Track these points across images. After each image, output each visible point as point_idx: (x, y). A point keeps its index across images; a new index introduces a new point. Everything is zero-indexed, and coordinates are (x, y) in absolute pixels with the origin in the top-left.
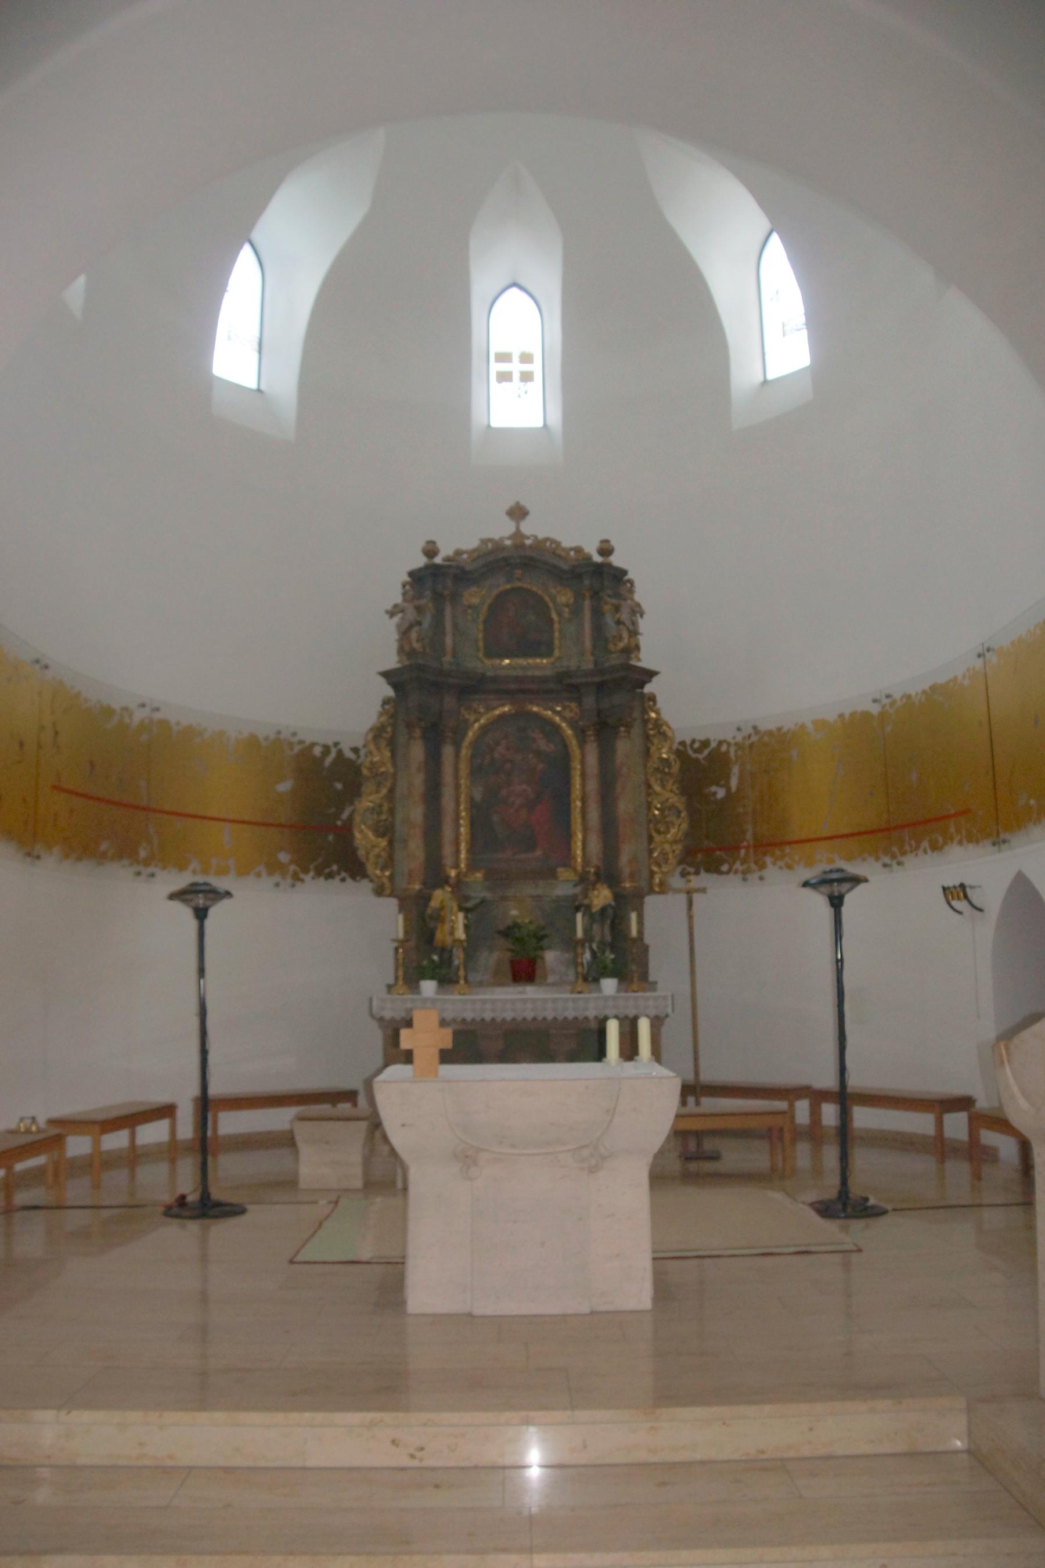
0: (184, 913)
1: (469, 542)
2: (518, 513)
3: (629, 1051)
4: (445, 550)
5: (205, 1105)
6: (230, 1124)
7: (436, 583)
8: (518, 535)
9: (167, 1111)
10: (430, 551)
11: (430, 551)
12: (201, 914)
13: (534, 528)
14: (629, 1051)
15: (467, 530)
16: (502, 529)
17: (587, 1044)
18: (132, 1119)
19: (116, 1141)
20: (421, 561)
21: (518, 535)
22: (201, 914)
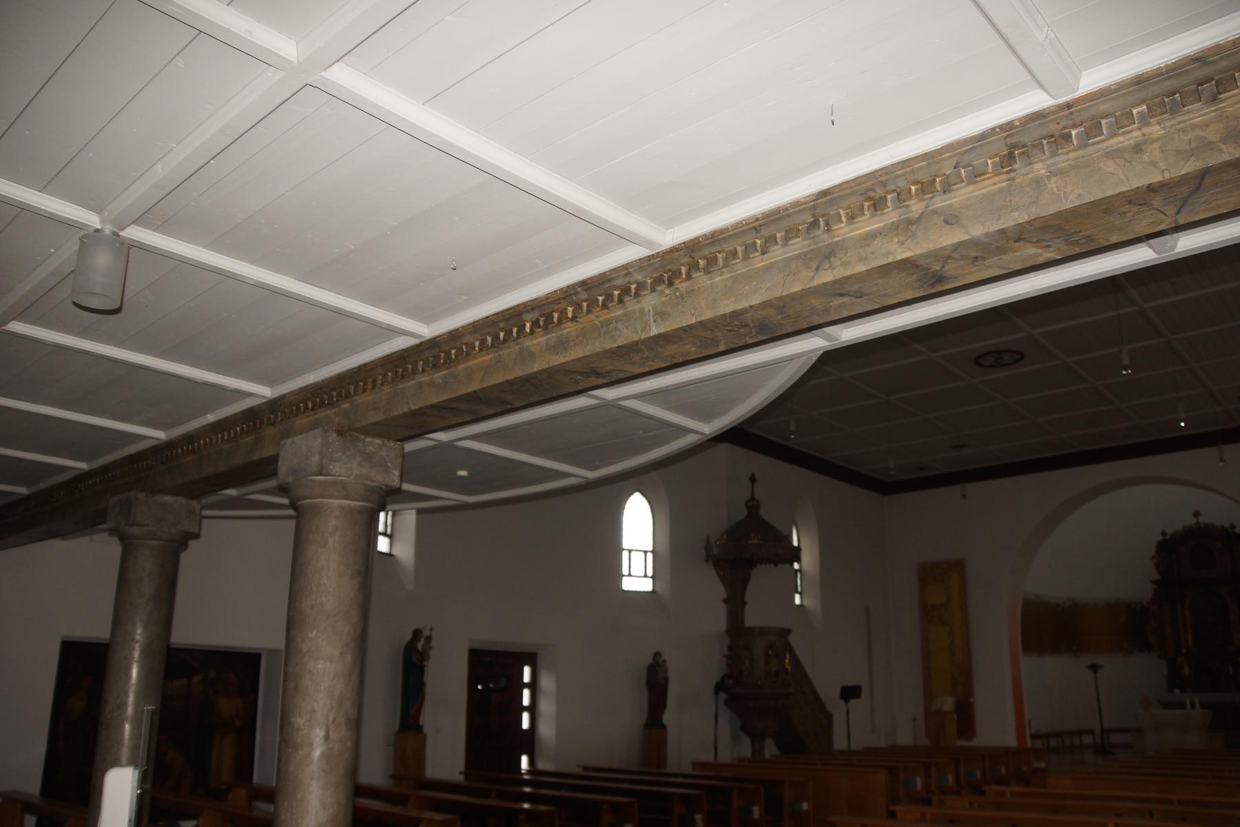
0: (1090, 673)
1: (1178, 527)
2: (1197, 514)
3: (1193, 706)
4: (1170, 531)
5: (1103, 730)
6: (1115, 738)
7: (1168, 547)
8: (1198, 523)
9: (1092, 732)
10: (1164, 533)
11: (1164, 533)
12: (1095, 672)
13: (1204, 519)
14: (1193, 706)
15: (1178, 521)
16: (1191, 521)
17: (1182, 706)
18: (1080, 733)
19: (1076, 741)
20: (1160, 538)
21: (1198, 523)
22: (1095, 672)
